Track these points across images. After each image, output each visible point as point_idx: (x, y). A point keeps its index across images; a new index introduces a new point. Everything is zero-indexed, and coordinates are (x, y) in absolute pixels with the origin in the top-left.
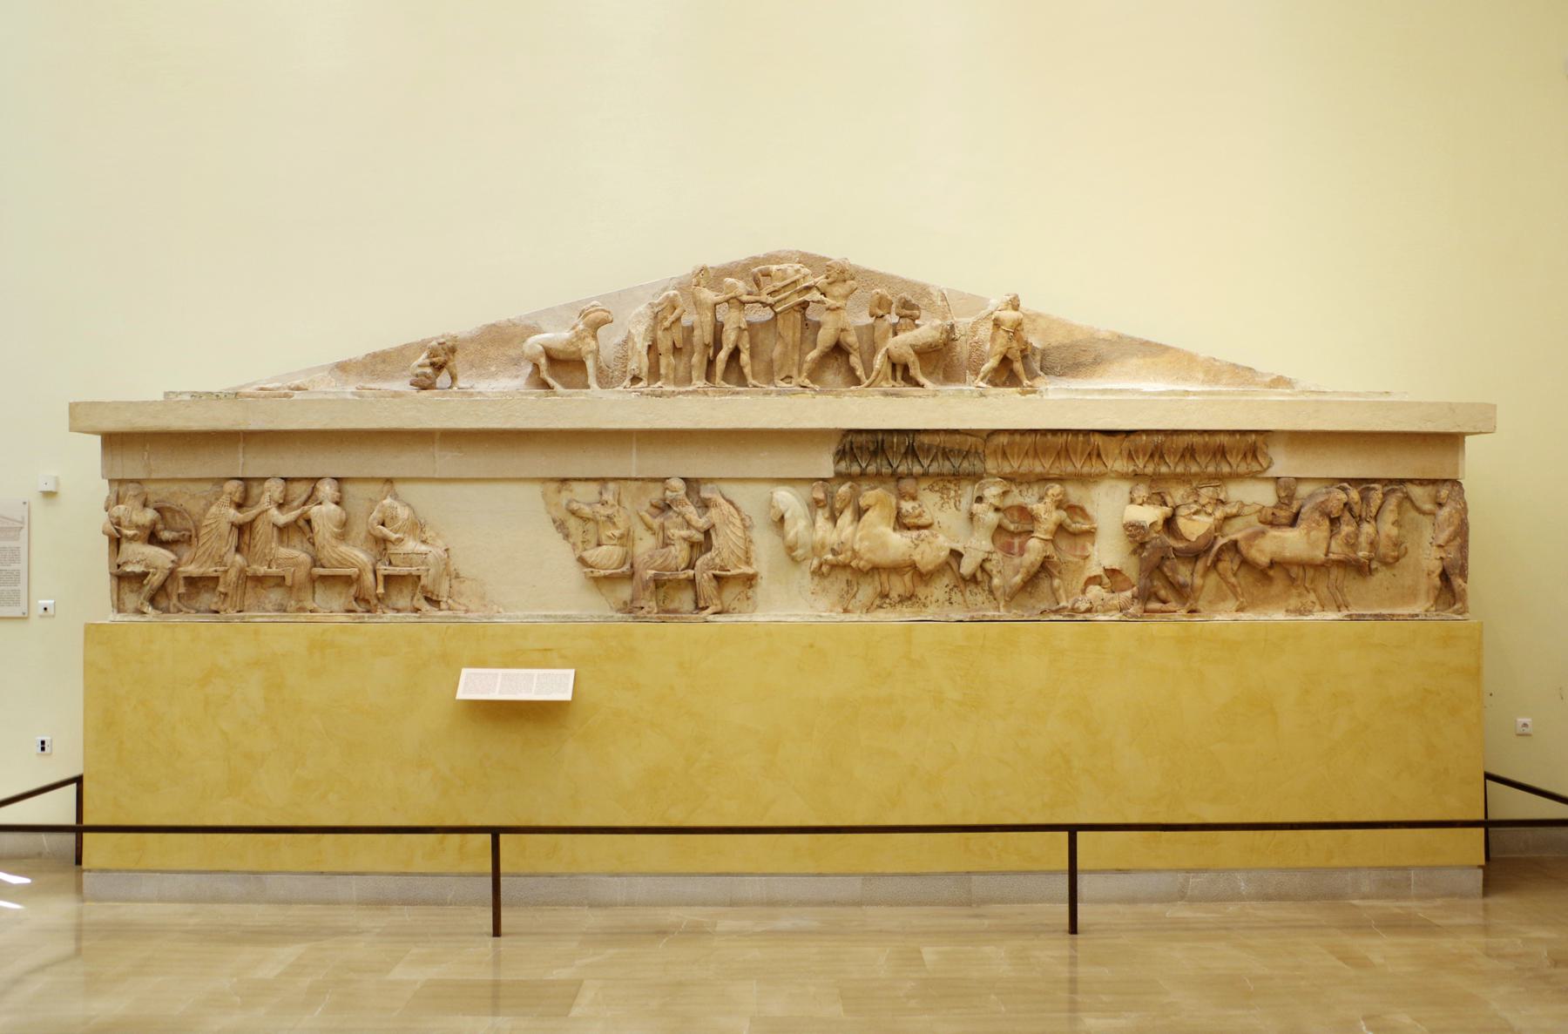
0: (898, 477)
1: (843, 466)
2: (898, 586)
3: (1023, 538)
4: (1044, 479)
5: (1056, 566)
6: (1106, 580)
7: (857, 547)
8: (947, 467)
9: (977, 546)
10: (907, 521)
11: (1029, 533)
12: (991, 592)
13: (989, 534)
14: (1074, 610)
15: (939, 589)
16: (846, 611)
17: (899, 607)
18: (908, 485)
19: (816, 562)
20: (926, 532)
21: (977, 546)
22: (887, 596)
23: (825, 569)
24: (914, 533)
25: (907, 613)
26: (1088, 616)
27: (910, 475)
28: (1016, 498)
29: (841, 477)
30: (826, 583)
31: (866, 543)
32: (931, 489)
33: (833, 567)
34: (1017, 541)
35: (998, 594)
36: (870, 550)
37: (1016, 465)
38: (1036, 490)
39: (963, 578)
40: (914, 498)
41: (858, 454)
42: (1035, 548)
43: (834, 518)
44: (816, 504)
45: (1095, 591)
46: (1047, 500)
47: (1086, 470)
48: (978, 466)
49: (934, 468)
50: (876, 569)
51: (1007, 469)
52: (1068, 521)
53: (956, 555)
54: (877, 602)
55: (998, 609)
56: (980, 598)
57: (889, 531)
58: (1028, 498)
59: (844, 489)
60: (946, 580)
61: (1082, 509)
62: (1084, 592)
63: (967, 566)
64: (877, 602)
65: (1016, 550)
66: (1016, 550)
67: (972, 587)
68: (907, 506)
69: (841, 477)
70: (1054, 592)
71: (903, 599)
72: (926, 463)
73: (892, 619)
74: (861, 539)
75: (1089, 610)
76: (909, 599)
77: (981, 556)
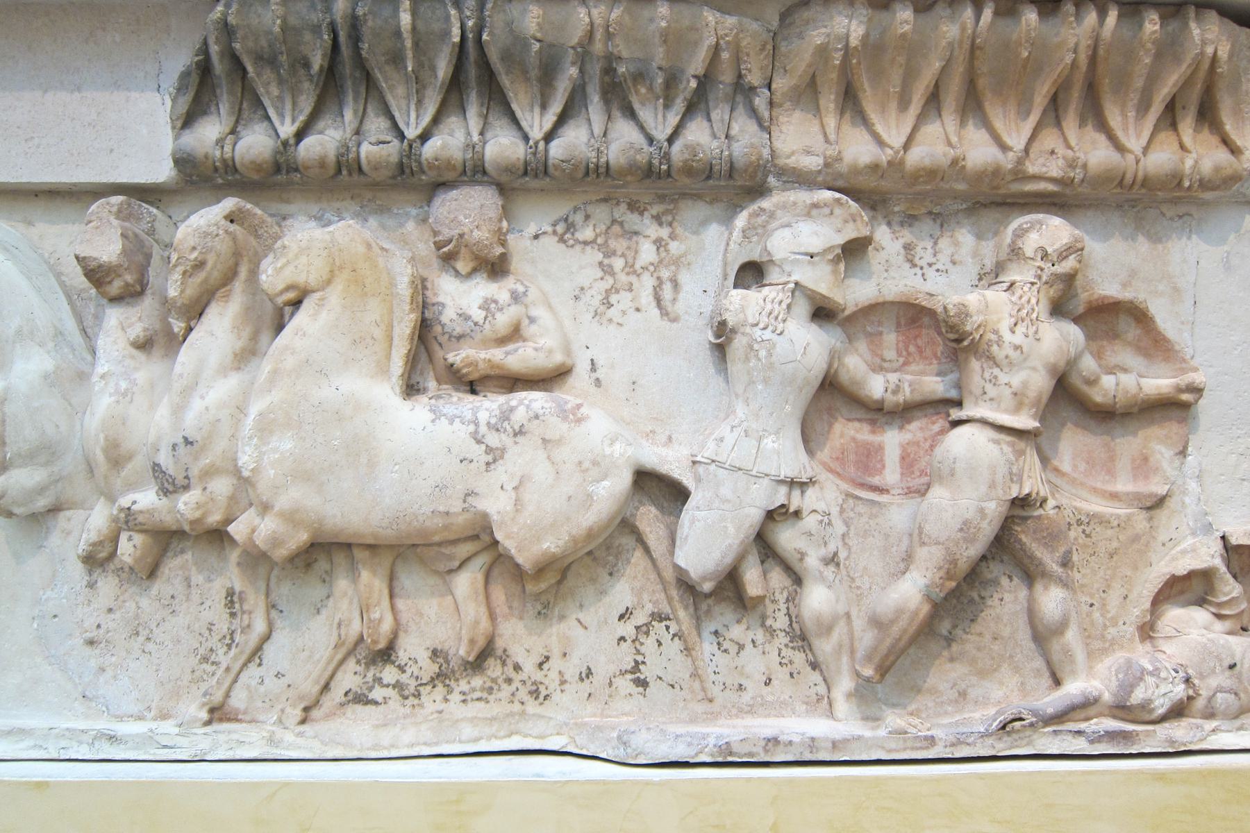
0: (415, 180)
1: (208, 134)
2: (438, 616)
3: (916, 429)
4: (997, 198)
5: (1052, 537)
6: (1230, 588)
7: (246, 460)
8: (623, 143)
9: (738, 454)
10: (458, 356)
11: (945, 408)
12: (801, 638)
13: (792, 411)
14: (1121, 710)
15: (592, 632)
16: (218, 713)
17: (432, 699)
18: (468, 211)
19: (95, 520)
20: (536, 399)
21: (738, 454)
22: (386, 655)
23: (129, 548)
24: (489, 405)
25: (466, 717)
26: (1181, 732)
27: (474, 172)
28: (892, 274)
29: (199, 178)
30: (146, 603)
31: (285, 444)
32: (566, 230)
33: (167, 539)
34: (892, 440)
35: (824, 647)
36: (302, 474)
37: (895, 136)
38: (964, 245)
39: (686, 585)
40: (496, 268)
41: (269, 91)
42: (974, 466)
43: (160, 342)
44: (109, 283)
45: (1191, 628)
46: (1020, 274)
47: (1161, 159)
48: (745, 139)
49: (575, 142)
50: (323, 553)
51: (858, 149)
52: (1088, 364)
53: (660, 490)
54: (349, 679)
55: (823, 704)
56: (755, 663)
57: (384, 393)
58: (944, 270)
59: (203, 222)
60: (622, 593)
61: (1139, 315)
62: (1147, 631)
63: (705, 539)
64: (349, 679)
65: (891, 475)
66: (891, 475)
67: (724, 615)
68: (461, 297)
69: (199, 178)
70: (1043, 636)
71: (445, 673)
72: (537, 124)
73: (398, 753)
74: (265, 428)
75: (1178, 711)
76: (478, 663)
77: (762, 497)
